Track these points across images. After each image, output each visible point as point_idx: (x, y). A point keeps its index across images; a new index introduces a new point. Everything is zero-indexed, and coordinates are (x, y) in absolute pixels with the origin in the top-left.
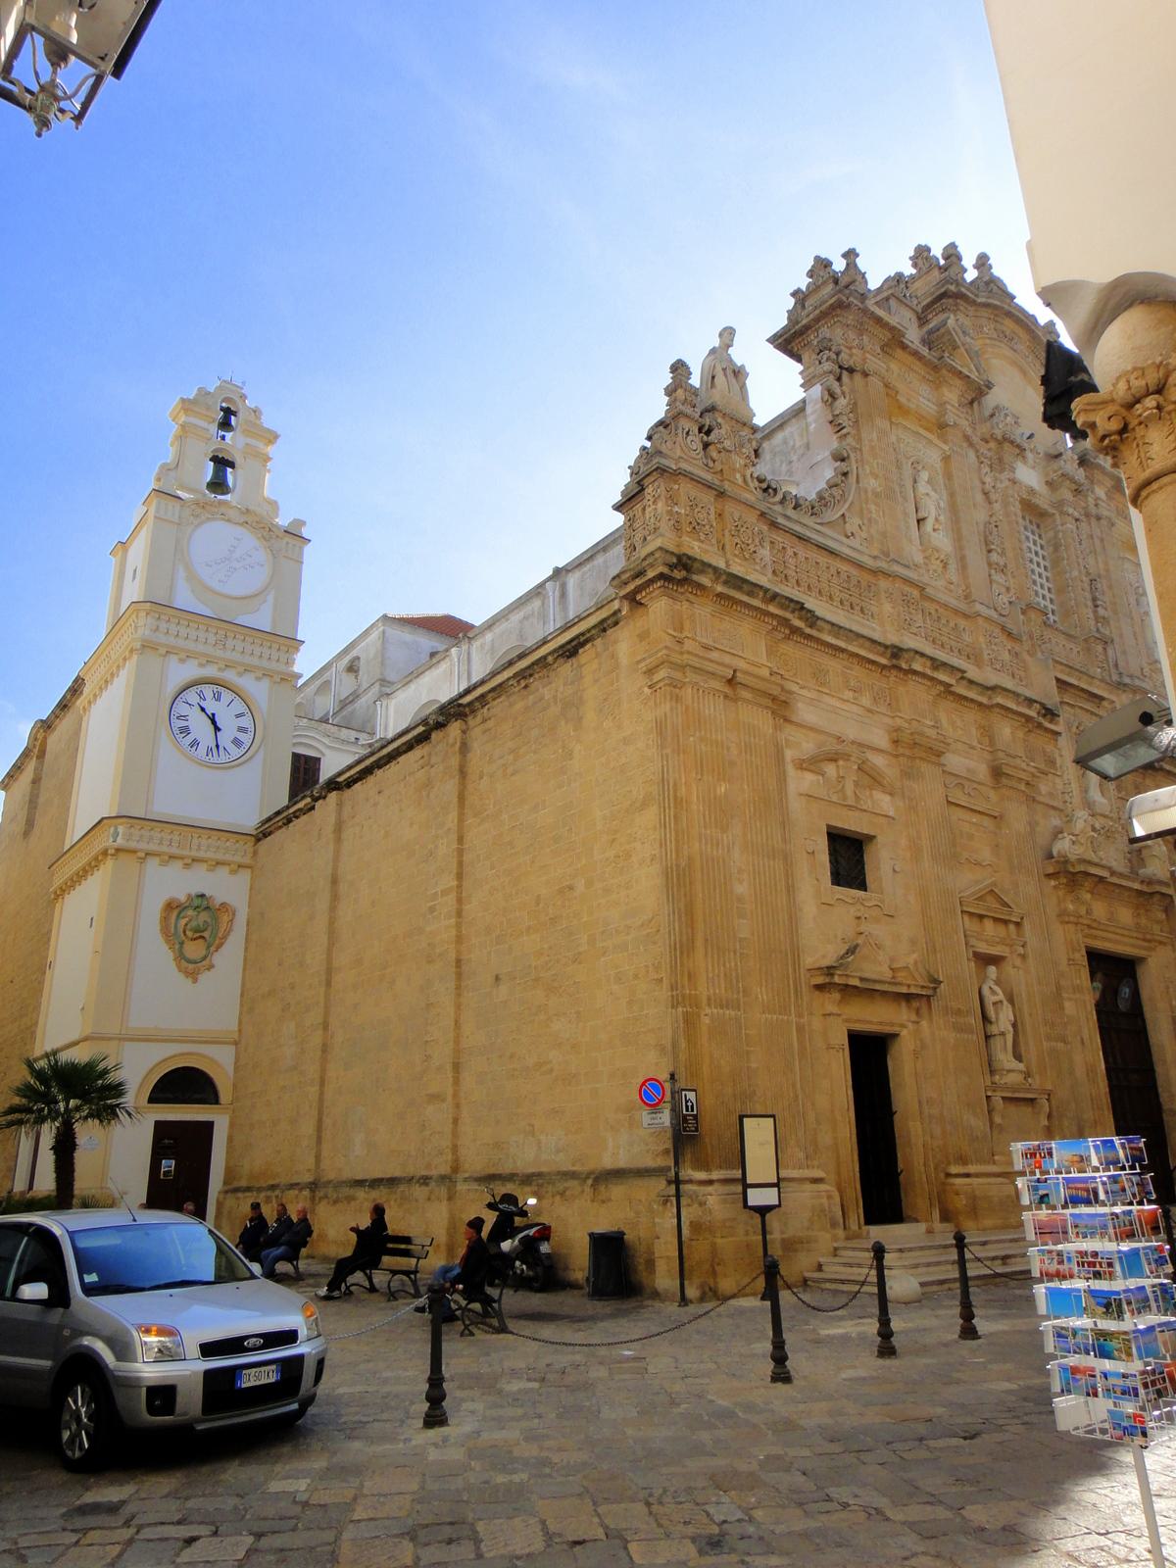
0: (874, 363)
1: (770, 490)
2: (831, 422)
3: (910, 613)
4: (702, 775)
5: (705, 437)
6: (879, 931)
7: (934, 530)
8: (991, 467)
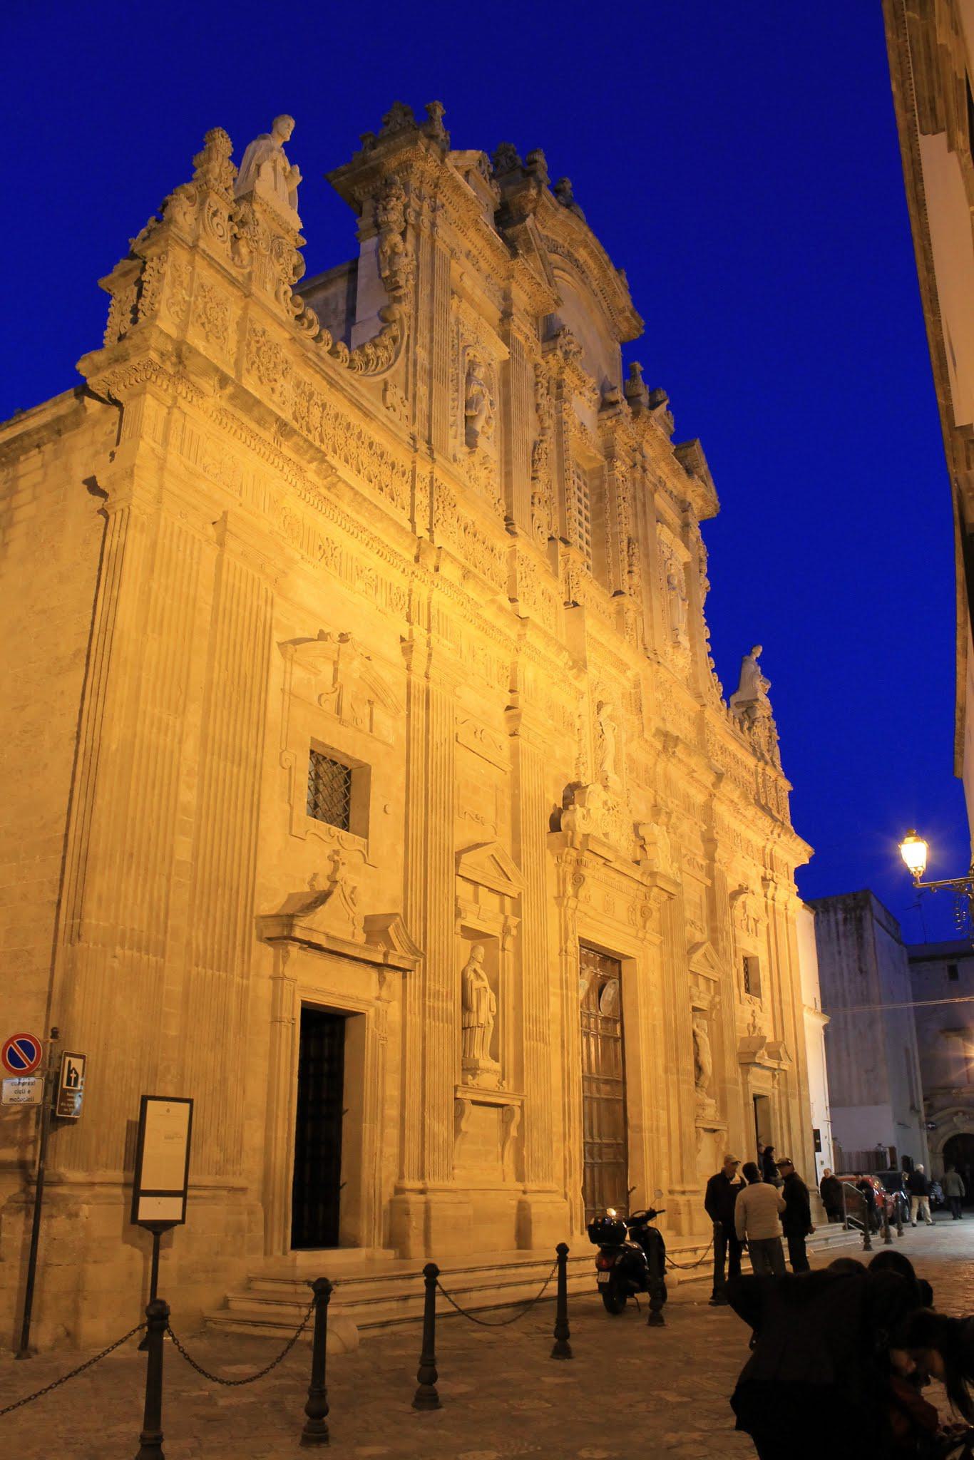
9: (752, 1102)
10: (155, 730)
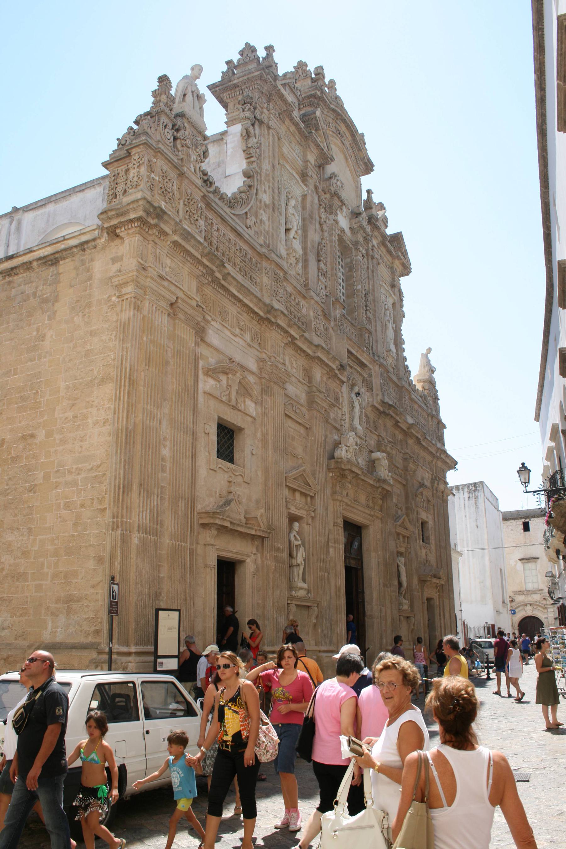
0: (274, 123)
1: (208, 183)
2: (244, 151)
3: (277, 287)
4: (149, 366)
5: (175, 133)
6: (241, 491)
7: (294, 238)
8: (325, 209)
9: (426, 601)
10: (148, 418)
